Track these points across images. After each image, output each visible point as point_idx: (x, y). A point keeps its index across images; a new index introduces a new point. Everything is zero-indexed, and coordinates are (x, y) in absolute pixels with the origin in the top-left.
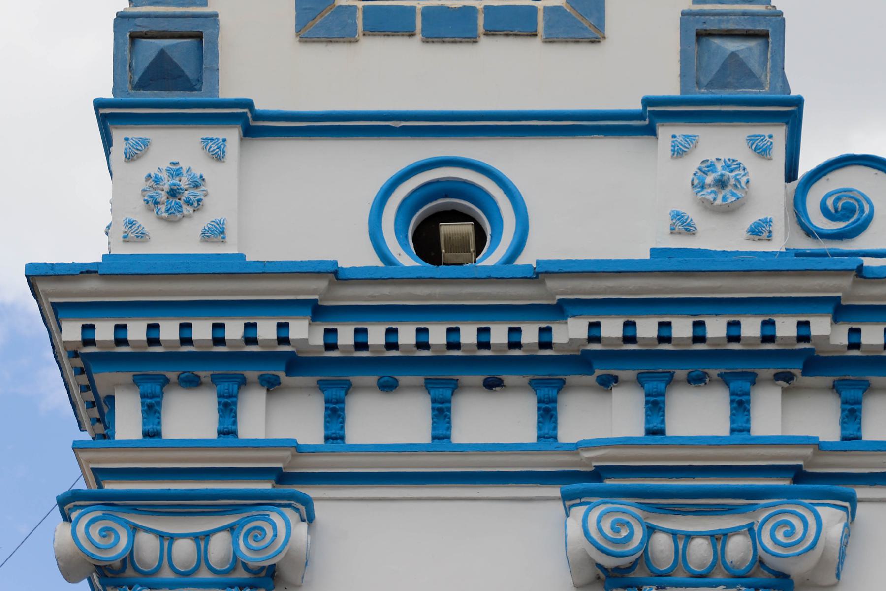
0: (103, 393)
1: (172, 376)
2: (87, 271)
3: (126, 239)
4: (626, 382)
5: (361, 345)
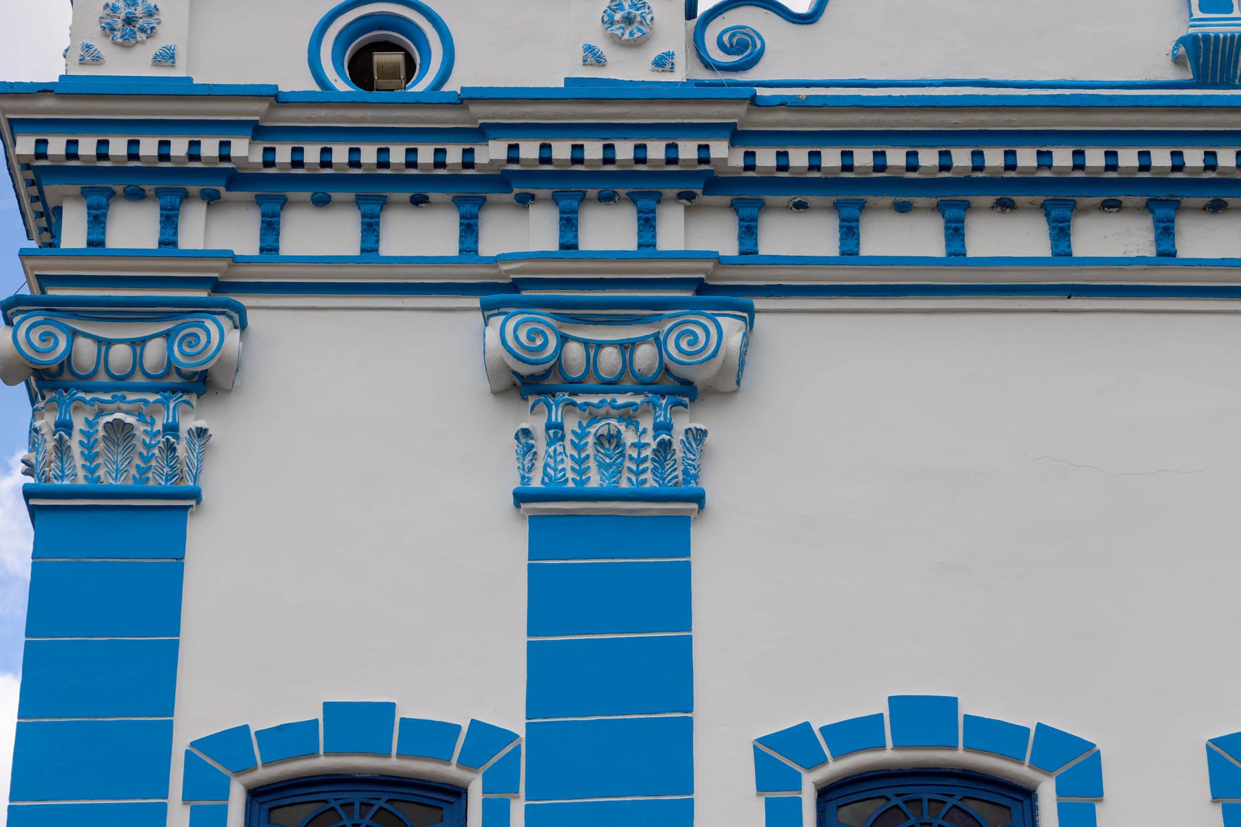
0: (51, 203)
1: (119, 189)
2: (44, 90)
3: (82, 62)
4: (542, 200)
5: (298, 163)
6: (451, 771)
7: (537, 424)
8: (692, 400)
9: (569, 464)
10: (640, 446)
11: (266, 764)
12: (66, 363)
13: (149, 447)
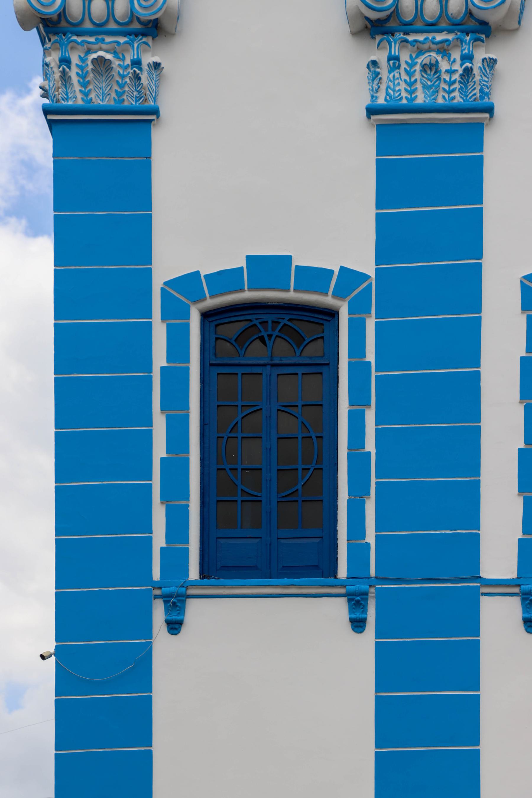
6: (328, 300)
7: (382, 57)
8: (487, 37)
9: (403, 86)
10: (451, 72)
11: (211, 297)
12: (63, 14)
13: (123, 77)
